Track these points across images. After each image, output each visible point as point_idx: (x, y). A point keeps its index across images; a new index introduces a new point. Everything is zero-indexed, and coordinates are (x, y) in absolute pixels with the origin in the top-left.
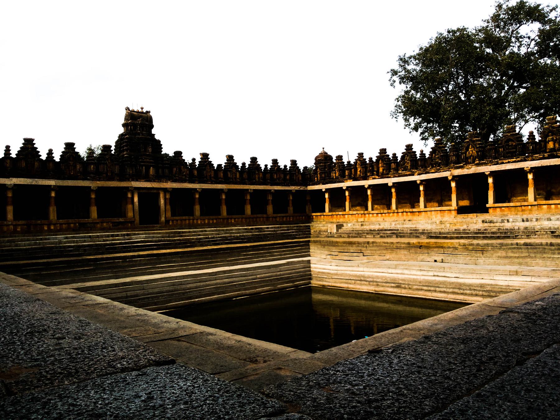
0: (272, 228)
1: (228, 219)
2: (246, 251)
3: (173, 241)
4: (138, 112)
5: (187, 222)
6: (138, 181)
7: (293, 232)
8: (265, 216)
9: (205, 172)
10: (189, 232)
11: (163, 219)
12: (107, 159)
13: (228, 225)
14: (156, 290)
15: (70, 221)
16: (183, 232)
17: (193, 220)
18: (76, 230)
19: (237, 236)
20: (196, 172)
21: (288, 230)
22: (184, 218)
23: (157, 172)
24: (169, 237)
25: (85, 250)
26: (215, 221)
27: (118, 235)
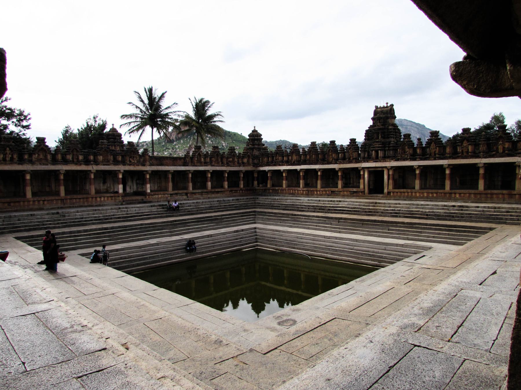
0: (485, 207)
1: (451, 193)
2: (397, 226)
3: (364, 209)
4: (384, 107)
5: (406, 194)
6: (368, 162)
7: (511, 216)
8: (505, 192)
9: (428, 150)
10: (385, 203)
11: (386, 191)
12: (350, 149)
13: (450, 199)
14: (284, 238)
15: (326, 189)
16: (379, 203)
17: (412, 193)
18: (329, 196)
19: (426, 212)
20: (418, 151)
21: (508, 212)
22: (402, 190)
23: (385, 154)
24: (364, 206)
25: (309, 208)
26: (435, 195)
27: (334, 201)
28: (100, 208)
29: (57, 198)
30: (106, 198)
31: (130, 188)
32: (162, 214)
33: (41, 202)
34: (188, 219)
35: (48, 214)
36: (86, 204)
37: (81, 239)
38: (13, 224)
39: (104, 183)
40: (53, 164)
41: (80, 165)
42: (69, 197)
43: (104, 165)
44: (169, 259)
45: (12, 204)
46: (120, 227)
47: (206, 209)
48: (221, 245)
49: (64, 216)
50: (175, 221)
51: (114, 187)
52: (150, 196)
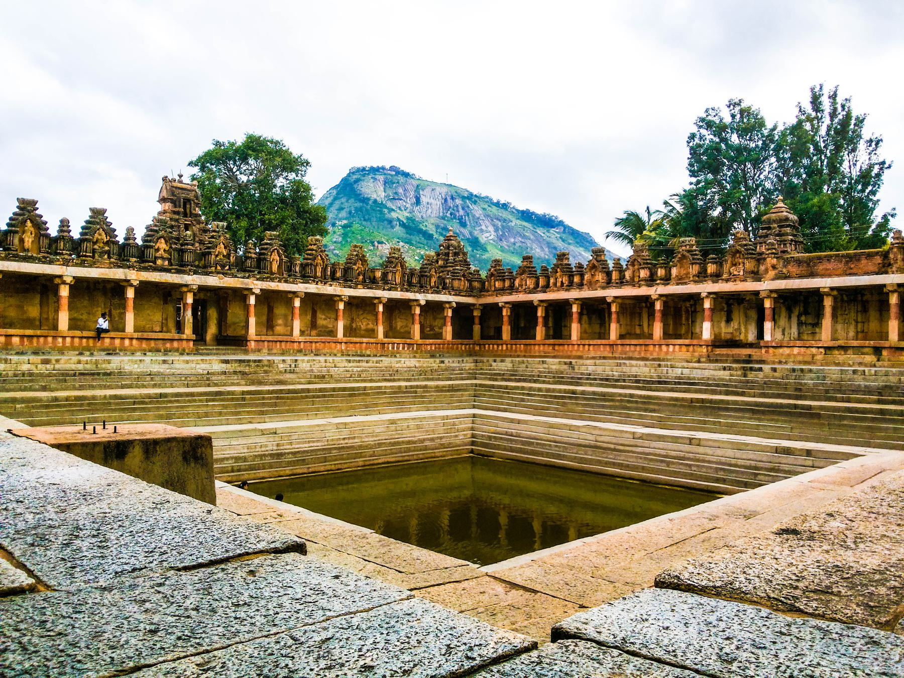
28: (627, 362)
29: (603, 342)
30: (677, 347)
31: (784, 334)
32: (736, 387)
33: (587, 347)
34: (735, 403)
35: (560, 363)
36: (643, 355)
37: (528, 400)
38: (516, 371)
39: (729, 320)
40: (603, 288)
41: (639, 287)
42: (619, 342)
43: (678, 284)
44: (559, 457)
45: (557, 348)
46: (594, 393)
47: (857, 390)
48: (690, 466)
49: (573, 368)
50: (703, 401)
51: (746, 328)
52: (771, 350)
